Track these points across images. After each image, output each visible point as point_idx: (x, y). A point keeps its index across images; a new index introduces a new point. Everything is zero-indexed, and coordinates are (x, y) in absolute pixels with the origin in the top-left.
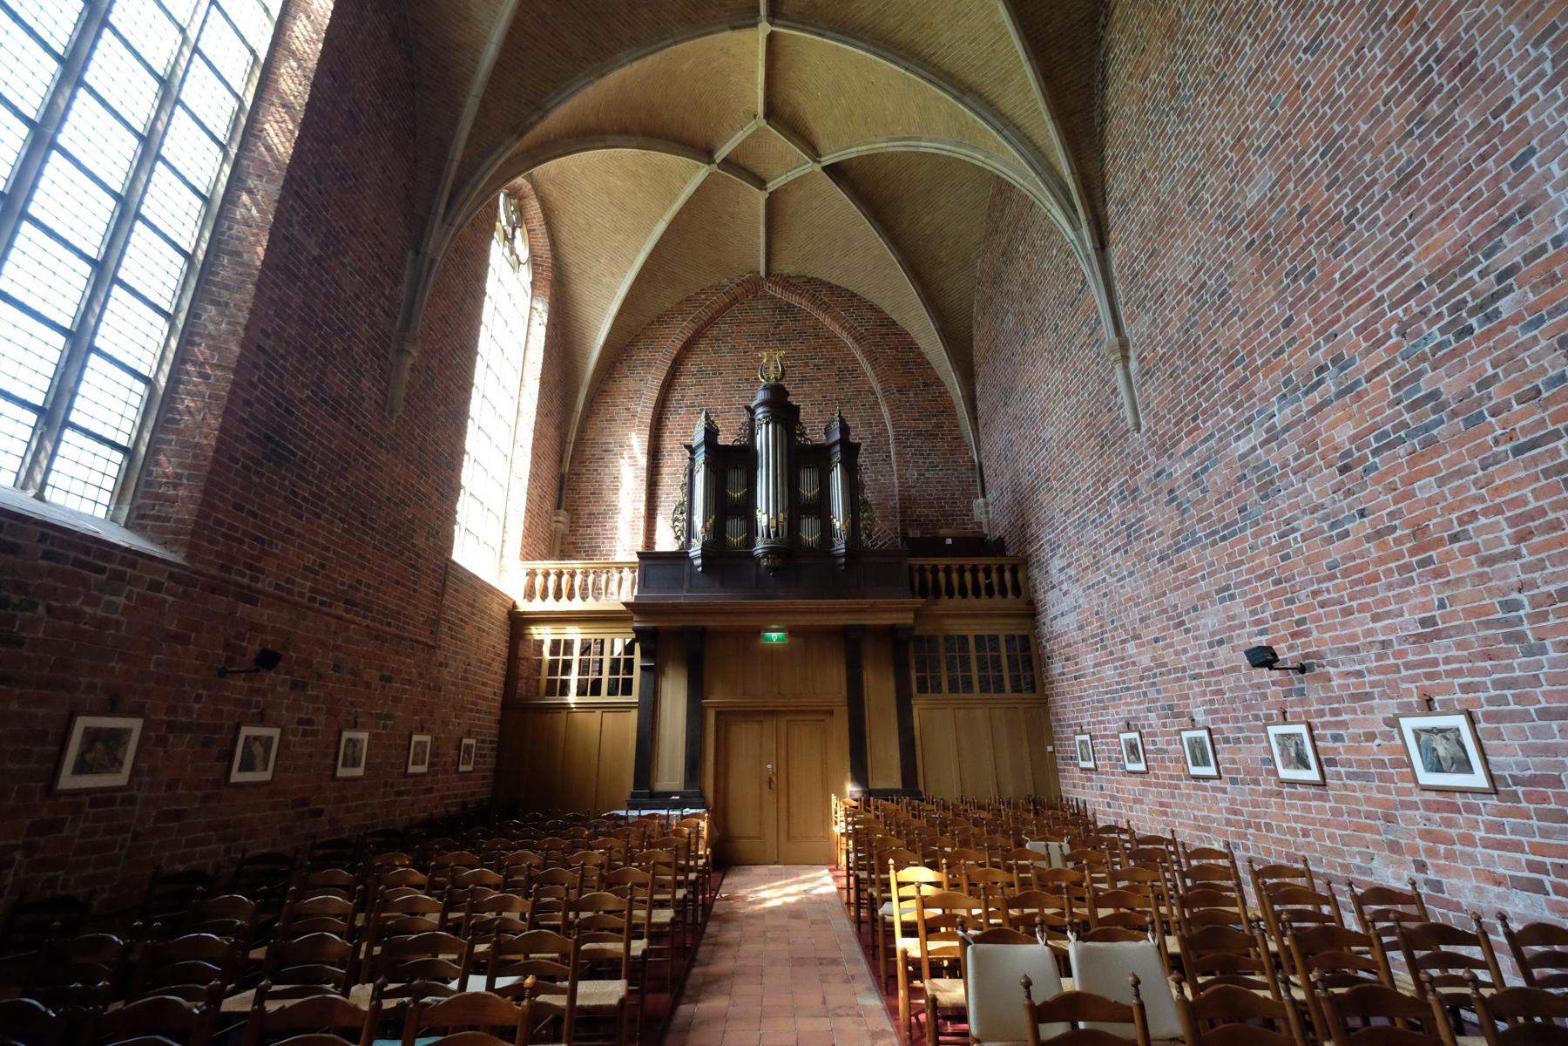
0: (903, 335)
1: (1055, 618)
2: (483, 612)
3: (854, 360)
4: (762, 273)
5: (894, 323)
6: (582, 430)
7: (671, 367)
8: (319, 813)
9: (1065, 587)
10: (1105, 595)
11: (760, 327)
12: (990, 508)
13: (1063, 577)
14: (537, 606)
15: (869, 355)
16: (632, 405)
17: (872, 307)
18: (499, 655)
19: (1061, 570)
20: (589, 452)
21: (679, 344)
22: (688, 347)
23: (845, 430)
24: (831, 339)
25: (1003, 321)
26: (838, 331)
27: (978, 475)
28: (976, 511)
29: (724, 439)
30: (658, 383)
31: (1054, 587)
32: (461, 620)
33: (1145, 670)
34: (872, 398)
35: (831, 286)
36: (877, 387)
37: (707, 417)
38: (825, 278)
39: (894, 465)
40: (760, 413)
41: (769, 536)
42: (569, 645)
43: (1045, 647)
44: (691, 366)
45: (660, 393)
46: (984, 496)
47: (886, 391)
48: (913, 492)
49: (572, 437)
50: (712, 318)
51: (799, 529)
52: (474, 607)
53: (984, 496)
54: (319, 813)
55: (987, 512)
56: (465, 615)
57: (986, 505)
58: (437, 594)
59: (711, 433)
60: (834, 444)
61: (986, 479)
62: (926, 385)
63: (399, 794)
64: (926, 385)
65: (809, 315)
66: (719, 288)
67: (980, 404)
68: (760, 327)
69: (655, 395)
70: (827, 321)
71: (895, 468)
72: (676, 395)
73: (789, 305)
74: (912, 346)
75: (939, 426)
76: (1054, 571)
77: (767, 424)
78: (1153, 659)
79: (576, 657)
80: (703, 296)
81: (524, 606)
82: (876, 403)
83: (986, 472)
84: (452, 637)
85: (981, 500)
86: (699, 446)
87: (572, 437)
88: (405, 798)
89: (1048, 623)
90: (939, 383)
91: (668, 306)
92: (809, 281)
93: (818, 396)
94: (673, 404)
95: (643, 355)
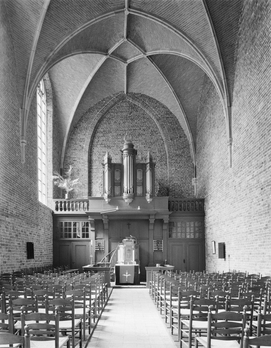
0: (174, 117)
1: (209, 217)
2: (46, 215)
3: (157, 127)
4: (125, 92)
5: (171, 113)
6: (66, 153)
7: (94, 130)
8: (24, 264)
9: (212, 208)
10: (220, 212)
11: (125, 114)
12: (197, 181)
13: (212, 206)
14: (59, 212)
15: (162, 125)
16: (81, 144)
17: (164, 107)
18: (51, 226)
19: (212, 204)
20: (69, 161)
21: (96, 121)
22: (100, 121)
23: (151, 159)
24: (149, 119)
25: (205, 118)
26: (151, 116)
27: (195, 169)
28: (193, 182)
29: (114, 161)
30: (90, 136)
31: (209, 208)
32: (43, 217)
33: (225, 232)
34: (162, 142)
35: (150, 98)
36: (164, 138)
37: (108, 154)
38: (147, 95)
39: (168, 166)
40: (125, 152)
41: (127, 193)
42: (70, 223)
43: (206, 225)
44: (100, 129)
45: (91, 140)
46: (196, 177)
47: (167, 139)
48: (173, 176)
49: (63, 156)
50: (108, 110)
51: (136, 190)
52: (44, 213)
53: (196, 177)
54: (24, 264)
55: (196, 182)
56: (43, 216)
57: (196, 180)
58: (36, 210)
59: (109, 160)
60: (147, 164)
61: (197, 171)
62: (180, 137)
63: (36, 261)
64: (180, 137)
65: (141, 109)
66: (110, 98)
67: (197, 145)
68: (125, 114)
69: (89, 140)
70: (148, 112)
71: (168, 167)
72: (96, 140)
73: (135, 105)
74: (177, 122)
75: (183, 152)
76: (210, 204)
77: (127, 156)
78: (227, 230)
79: (72, 227)
80: (104, 102)
81: (56, 212)
82: (163, 143)
83: (197, 169)
84: (41, 222)
85: (195, 178)
86: (106, 164)
87: (63, 156)
88: (37, 262)
89: (207, 218)
90: (185, 136)
91: (92, 105)
92: (142, 95)
93: (144, 141)
94: (95, 143)
95: (84, 125)
